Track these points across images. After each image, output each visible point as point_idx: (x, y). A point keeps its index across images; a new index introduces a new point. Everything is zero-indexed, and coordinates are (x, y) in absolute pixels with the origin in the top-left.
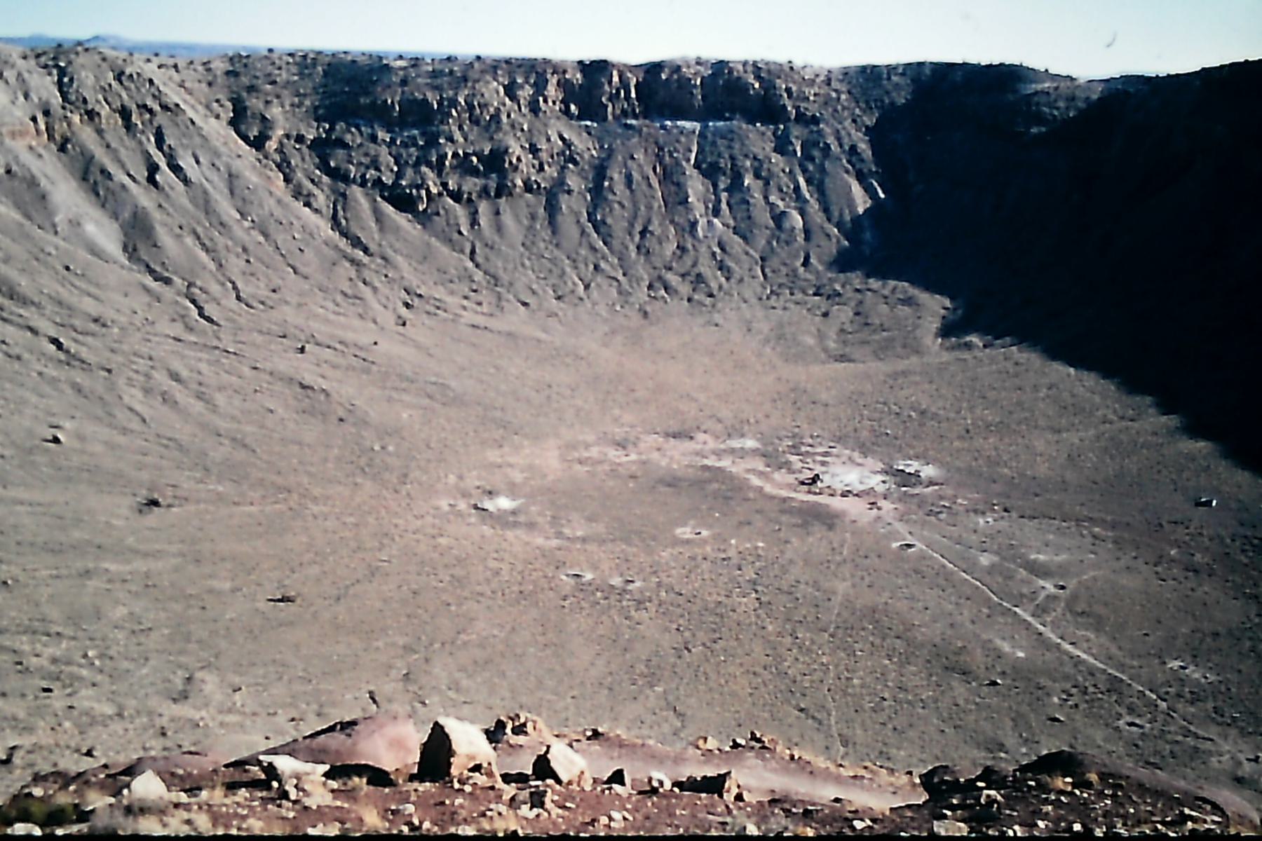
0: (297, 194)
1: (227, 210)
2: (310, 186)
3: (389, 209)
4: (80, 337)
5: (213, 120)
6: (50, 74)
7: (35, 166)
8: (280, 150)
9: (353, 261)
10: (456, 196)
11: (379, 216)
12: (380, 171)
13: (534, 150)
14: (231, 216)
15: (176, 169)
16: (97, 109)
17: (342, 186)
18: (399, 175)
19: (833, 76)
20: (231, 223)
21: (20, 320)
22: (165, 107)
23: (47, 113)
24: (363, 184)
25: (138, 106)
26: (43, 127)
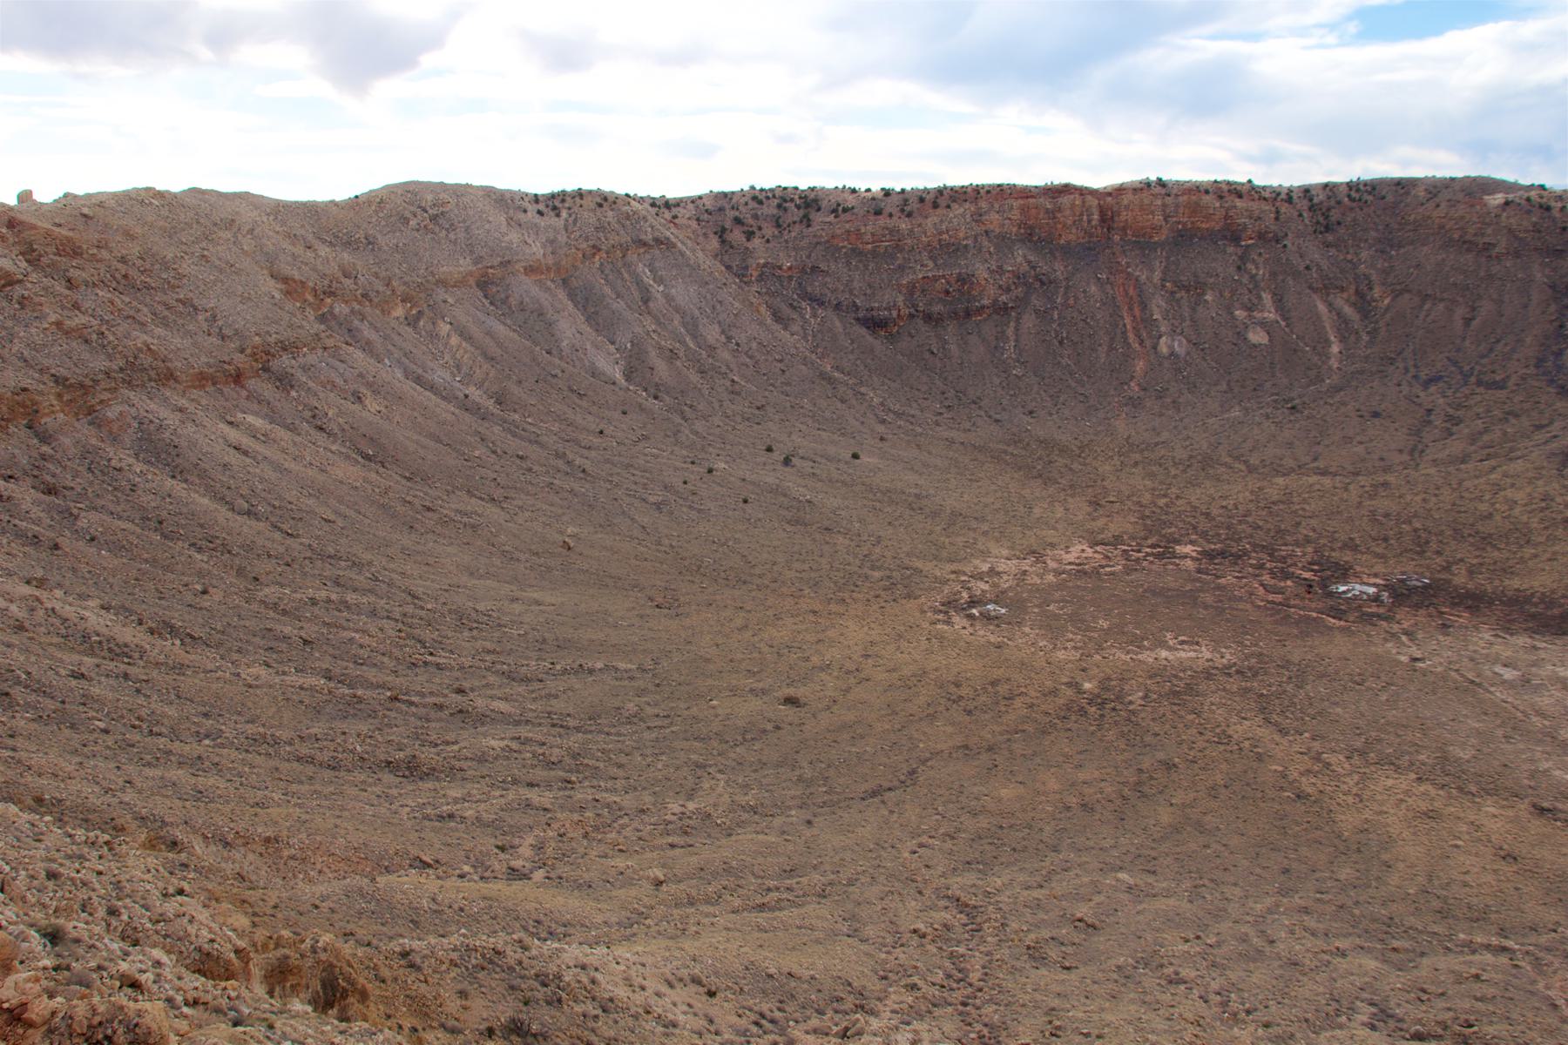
0: (778, 317)
1: (712, 334)
3: (863, 331)
4: (585, 452)
5: (700, 254)
6: (558, 215)
7: (545, 299)
8: (761, 278)
10: (928, 318)
13: (1000, 270)
15: (669, 299)
19: (1295, 196)
21: (532, 437)
22: (658, 241)
24: (838, 307)
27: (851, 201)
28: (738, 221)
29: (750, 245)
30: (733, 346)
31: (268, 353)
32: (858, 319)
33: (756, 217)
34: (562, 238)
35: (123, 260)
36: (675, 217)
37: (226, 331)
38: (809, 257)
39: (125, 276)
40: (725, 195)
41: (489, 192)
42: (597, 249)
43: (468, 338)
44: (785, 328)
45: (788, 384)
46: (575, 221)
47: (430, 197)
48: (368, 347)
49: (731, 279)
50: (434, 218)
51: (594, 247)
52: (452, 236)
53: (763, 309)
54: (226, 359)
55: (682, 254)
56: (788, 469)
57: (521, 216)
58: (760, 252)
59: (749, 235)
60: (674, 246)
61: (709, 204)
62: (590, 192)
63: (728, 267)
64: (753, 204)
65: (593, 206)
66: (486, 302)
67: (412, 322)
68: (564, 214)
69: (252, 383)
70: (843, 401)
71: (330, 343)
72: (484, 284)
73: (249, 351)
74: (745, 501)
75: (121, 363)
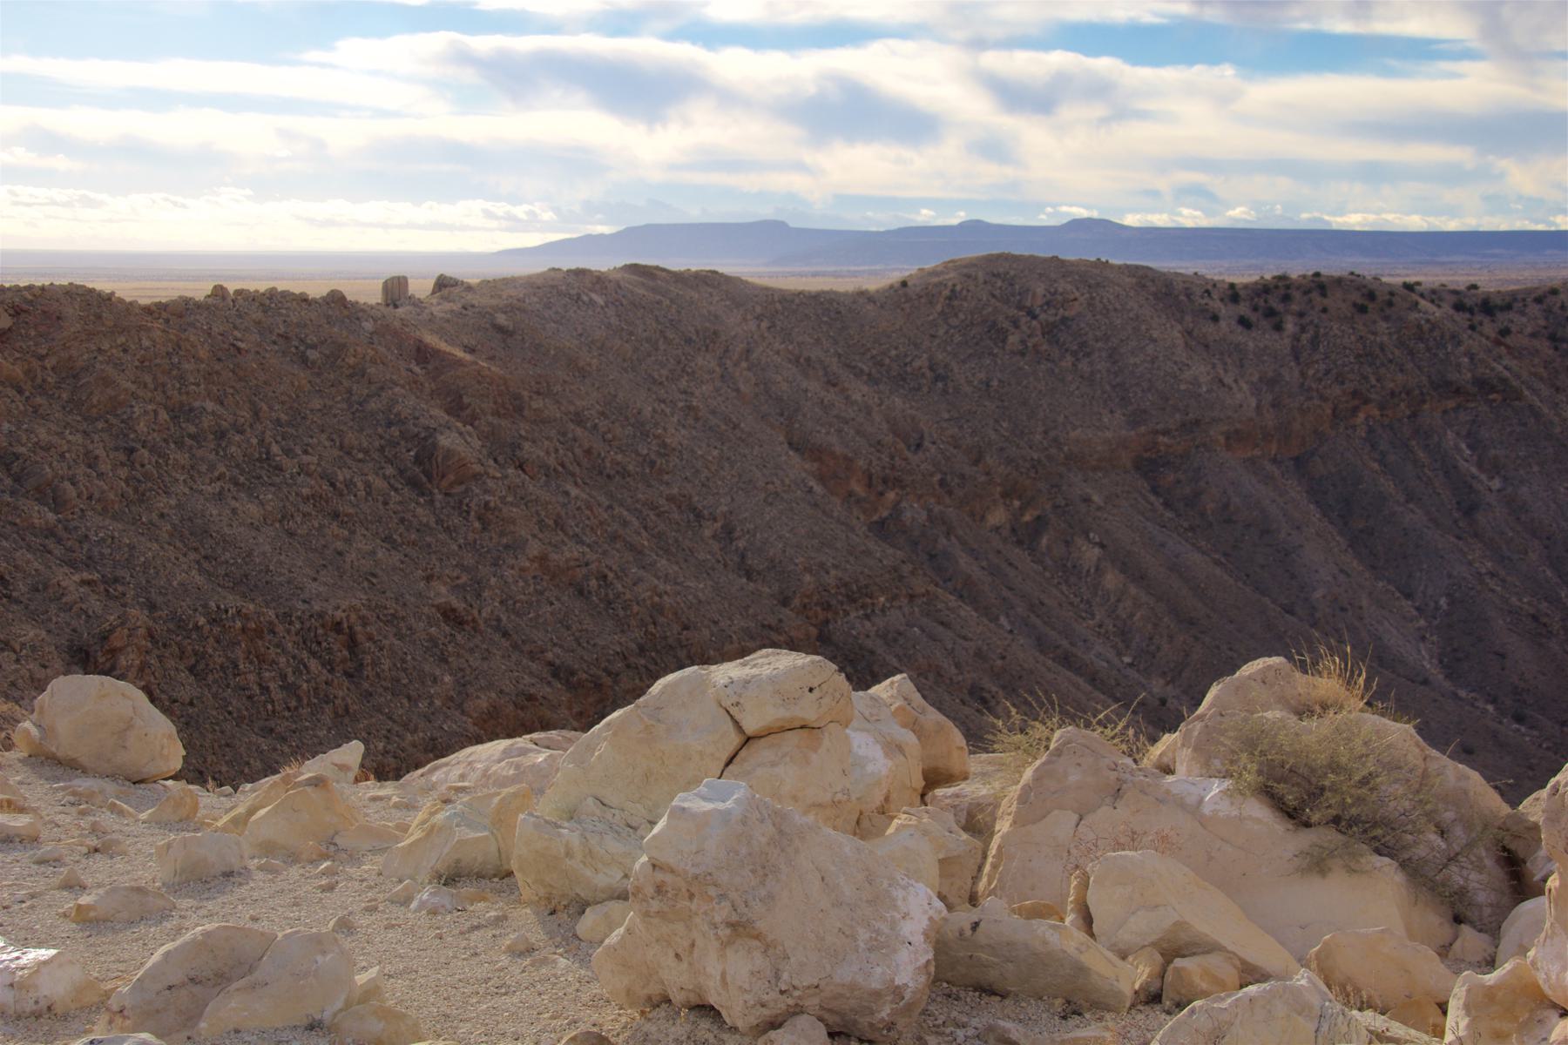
22: (1484, 386)
31: (827, 607)
34: (1291, 374)
35: (579, 419)
36: (1505, 332)
37: (753, 561)
39: (588, 452)
41: (1143, 278)
42: (1359, 398)
43: (1141, 578)
46: (1315, 342)
47: (1040, 290)
48: (967, 592)
50: (1049, 331)
51: (1355, 394)
52: (1084, 366)
54: (772, 620)
55: (1537, 415)
57: (1209, 328)
62: (1339, 281)
66: (1157, 502)
67: (1026, 536)
68: (1290, 326)
72: (1149, 466)
73: (796, 602)
75: (638, 634)
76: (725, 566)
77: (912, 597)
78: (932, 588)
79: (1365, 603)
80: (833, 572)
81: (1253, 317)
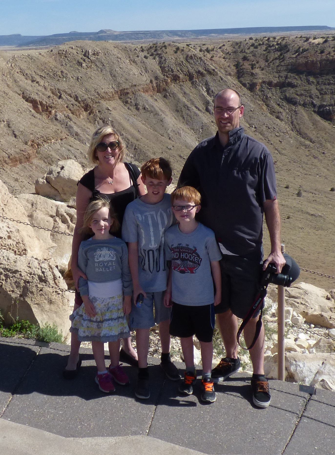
0: (272, 112)
2: (278, 107)
3: (318, 118)
5: (229, 77)
6: (154, 59)
9: (306, 146)
11: (315, 123)
12: (312, 98)
14: (245, 126)
16: (178, 74)
17: (294, 107)
18: (323, 100)
20: (246, 129)
23: (157, 78)
24: (304, 105)
25: (196, 72)
26: (155, 85)
27: (306, 45)
28: (245, 59)
29: (254, 71)
30: (253, 129)
32: (315, 112)
33: (254, 56)
38: (286, 77)
40: (237, 44)
44: (278, 117)
45: (285, 149)
49: (245, 89)
53: (265, 107)
56: (301, 198)
58: (261, 76)
59: (253, 66)
60: (217, 74)
61: (229, 49)
63: (244, 85)
64: (252, 49)
65: (172, 52)
69: (35, 161)
70: (315, 158)
71: (64, 135)
73: (29, 143)
74: (288, 218)
76: (8, 134)
77: (61, 140)
78: (66, 136)
79: (181, 132)
80: (39, 134)
81: (148, 55)
